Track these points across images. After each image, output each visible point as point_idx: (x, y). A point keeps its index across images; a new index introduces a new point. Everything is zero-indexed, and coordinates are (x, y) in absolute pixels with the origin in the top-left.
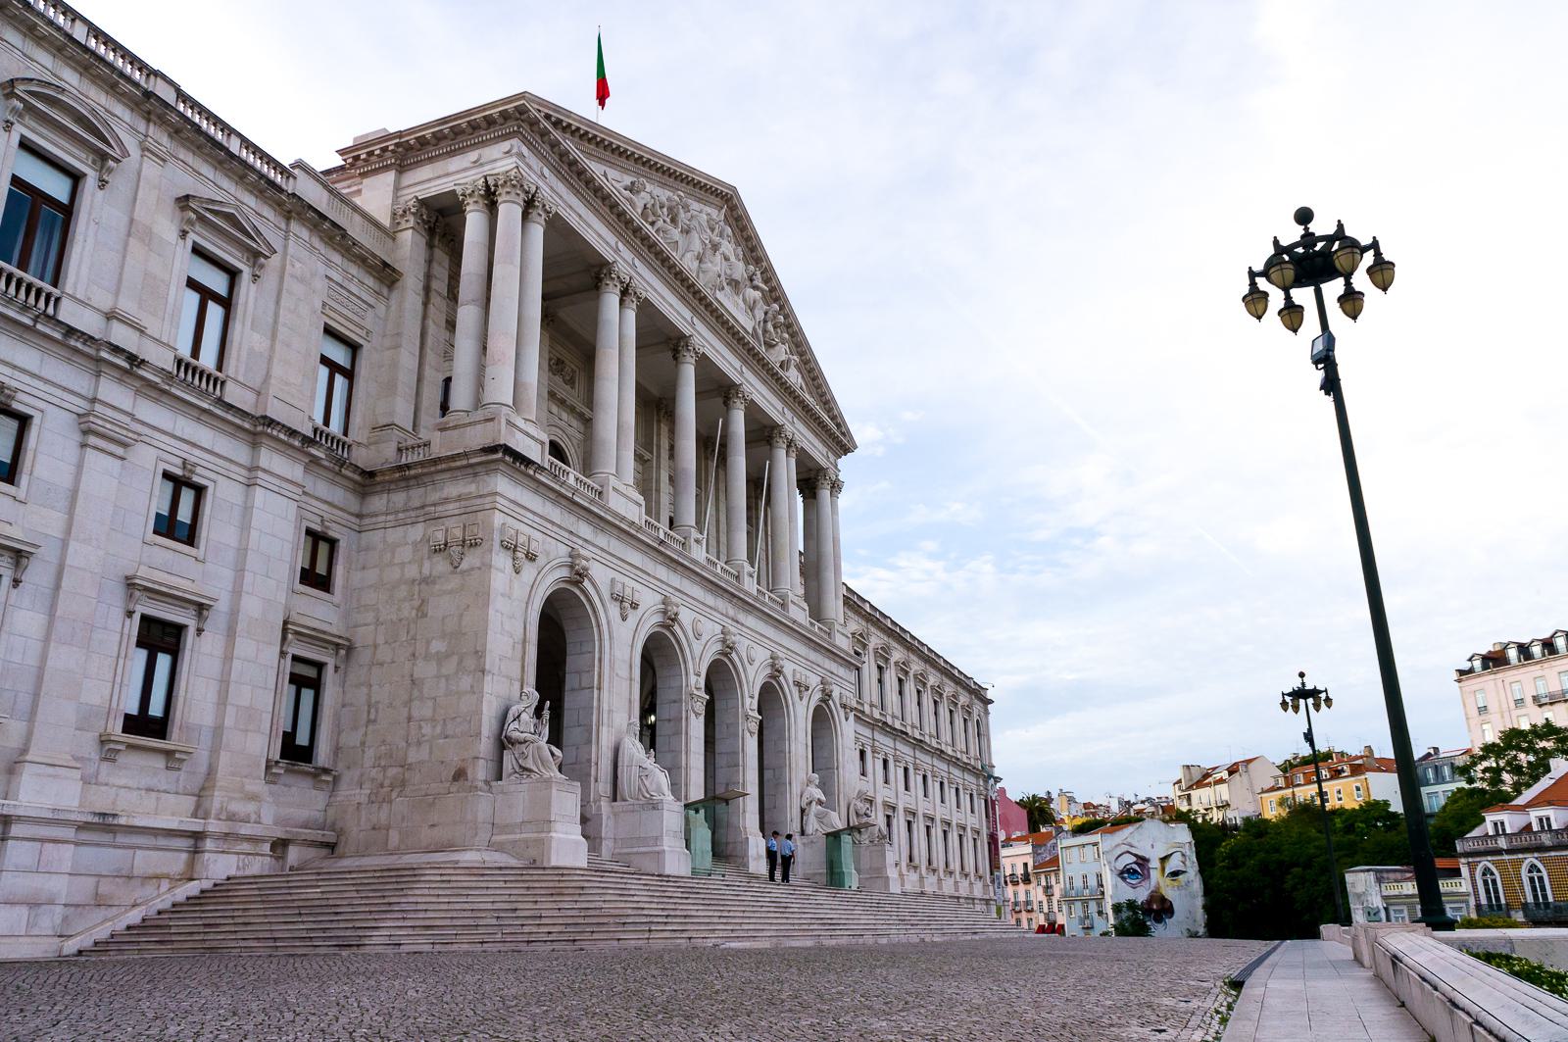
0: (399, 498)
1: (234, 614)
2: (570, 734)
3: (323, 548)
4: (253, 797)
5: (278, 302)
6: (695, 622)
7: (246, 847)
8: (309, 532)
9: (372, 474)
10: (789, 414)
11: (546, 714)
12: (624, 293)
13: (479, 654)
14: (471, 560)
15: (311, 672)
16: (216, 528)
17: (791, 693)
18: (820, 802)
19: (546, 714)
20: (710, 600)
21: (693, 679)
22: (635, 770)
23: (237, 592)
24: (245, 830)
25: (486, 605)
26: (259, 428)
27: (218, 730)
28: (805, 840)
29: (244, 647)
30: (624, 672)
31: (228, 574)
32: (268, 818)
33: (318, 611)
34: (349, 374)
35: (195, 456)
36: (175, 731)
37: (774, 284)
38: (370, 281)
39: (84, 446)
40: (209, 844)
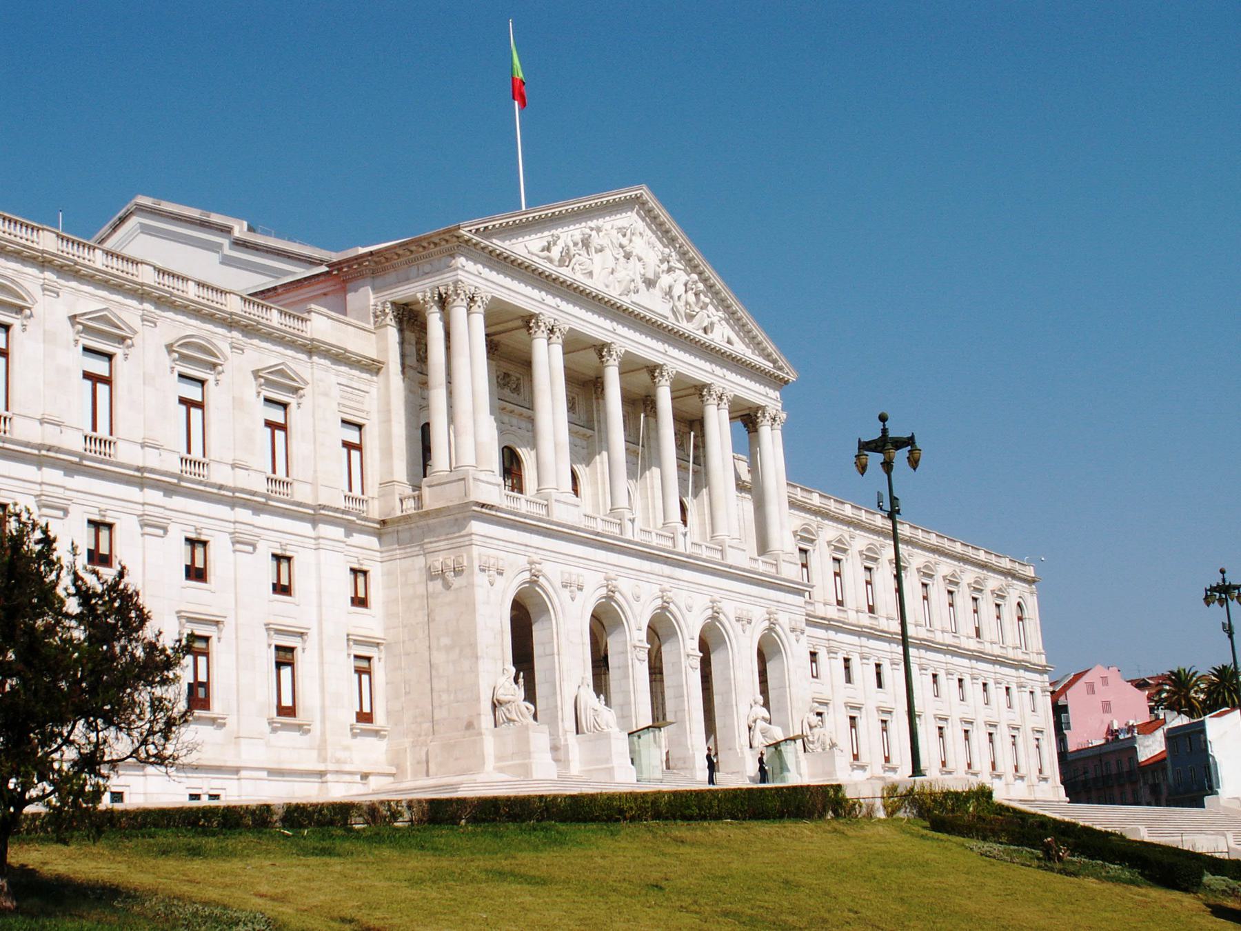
1: (321, 632)
4: (347, 748)
7: (347, 778)
11: (521, 681)
12: (551, 331)
13: (473, 645)
16: (301, 582)
17: (732, 629)
18: (764, 719)
19: (521, 681)
24: (347, 768)
25: (474, 611)
26: (316, 515)
27: (323, 708)
34: (359, 448)
36: (299, 711)
39: (235, 551)
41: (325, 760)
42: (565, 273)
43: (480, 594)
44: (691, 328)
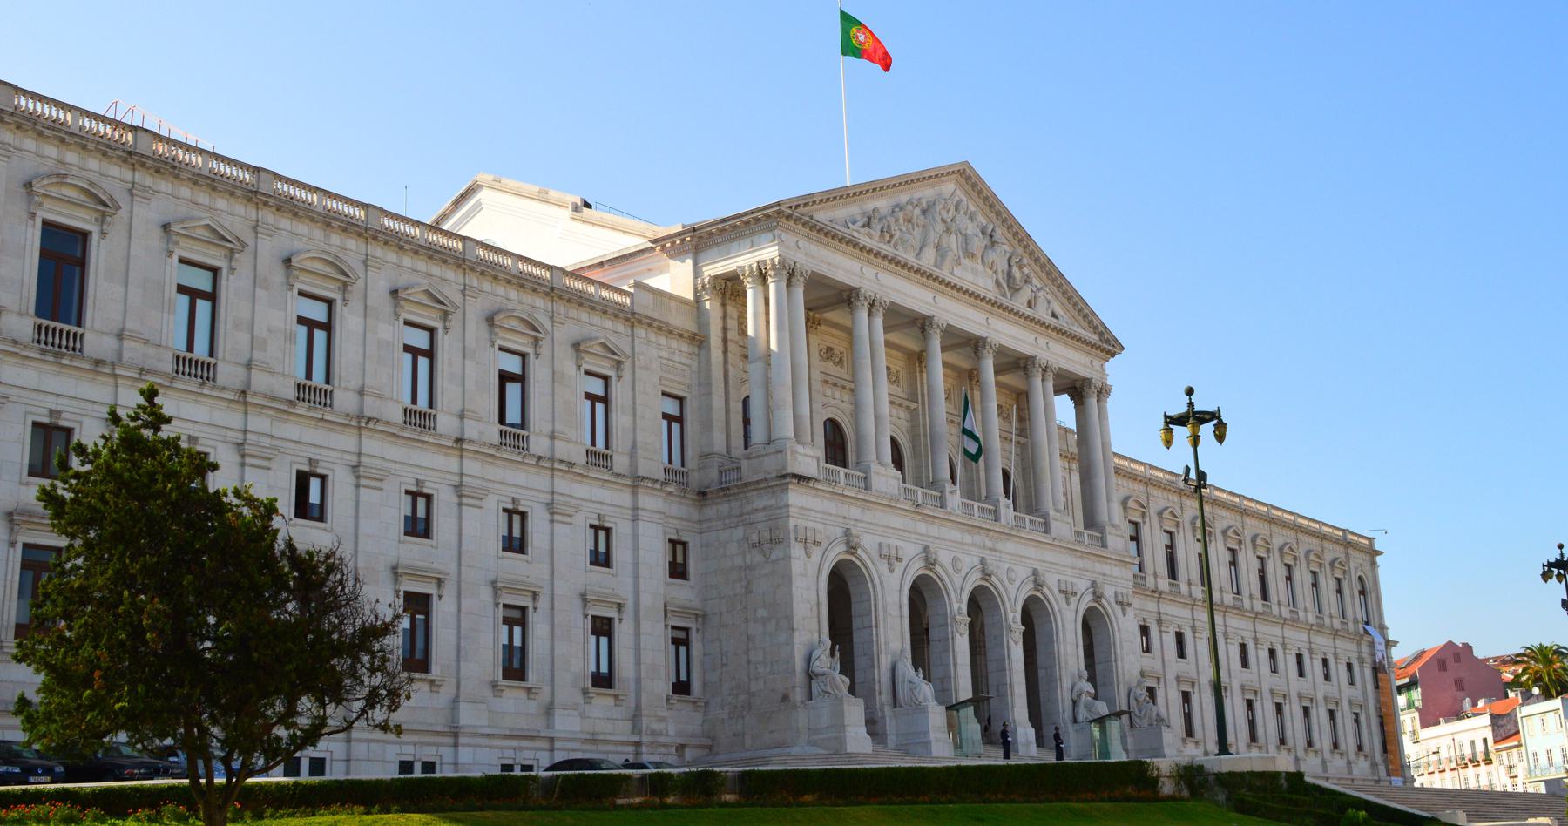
0: (724, 508)
2: (860, 662)
3: (679, 548)
4: (662, 720)
5: (633, 389)
6: (955, 560)
8: (670, 541)
9: (704, 494)
10: (1042, 341)
13: (789, 618)
14: (777, 553)
15: (682, 635)
16: (620, 554)
19: (837, 654)
20: (968, 538)
21: (956, 606)
22: (907, 686)
23: (637, 593)
24: (662, 740)
27: (638, 680)
28: (1077, 727)
29: (645, 626)
30: (895, 612)
31: (630, 581)
32: (672, 732)
33: (683, 593)
35: (604, 510)
36: (617, 683)
37: (1016, 228)
38: (685, 348)
40: (644, 749)
41: (640, 733)
42: (887, 249)
43: (797, 566)
44: (1020, 303)
